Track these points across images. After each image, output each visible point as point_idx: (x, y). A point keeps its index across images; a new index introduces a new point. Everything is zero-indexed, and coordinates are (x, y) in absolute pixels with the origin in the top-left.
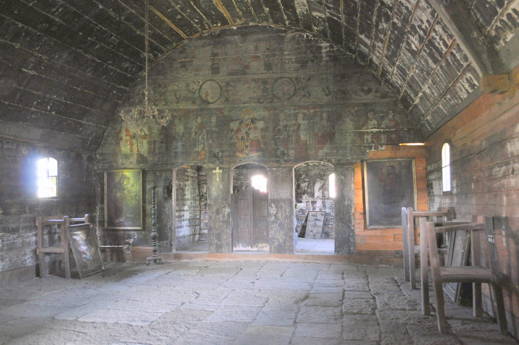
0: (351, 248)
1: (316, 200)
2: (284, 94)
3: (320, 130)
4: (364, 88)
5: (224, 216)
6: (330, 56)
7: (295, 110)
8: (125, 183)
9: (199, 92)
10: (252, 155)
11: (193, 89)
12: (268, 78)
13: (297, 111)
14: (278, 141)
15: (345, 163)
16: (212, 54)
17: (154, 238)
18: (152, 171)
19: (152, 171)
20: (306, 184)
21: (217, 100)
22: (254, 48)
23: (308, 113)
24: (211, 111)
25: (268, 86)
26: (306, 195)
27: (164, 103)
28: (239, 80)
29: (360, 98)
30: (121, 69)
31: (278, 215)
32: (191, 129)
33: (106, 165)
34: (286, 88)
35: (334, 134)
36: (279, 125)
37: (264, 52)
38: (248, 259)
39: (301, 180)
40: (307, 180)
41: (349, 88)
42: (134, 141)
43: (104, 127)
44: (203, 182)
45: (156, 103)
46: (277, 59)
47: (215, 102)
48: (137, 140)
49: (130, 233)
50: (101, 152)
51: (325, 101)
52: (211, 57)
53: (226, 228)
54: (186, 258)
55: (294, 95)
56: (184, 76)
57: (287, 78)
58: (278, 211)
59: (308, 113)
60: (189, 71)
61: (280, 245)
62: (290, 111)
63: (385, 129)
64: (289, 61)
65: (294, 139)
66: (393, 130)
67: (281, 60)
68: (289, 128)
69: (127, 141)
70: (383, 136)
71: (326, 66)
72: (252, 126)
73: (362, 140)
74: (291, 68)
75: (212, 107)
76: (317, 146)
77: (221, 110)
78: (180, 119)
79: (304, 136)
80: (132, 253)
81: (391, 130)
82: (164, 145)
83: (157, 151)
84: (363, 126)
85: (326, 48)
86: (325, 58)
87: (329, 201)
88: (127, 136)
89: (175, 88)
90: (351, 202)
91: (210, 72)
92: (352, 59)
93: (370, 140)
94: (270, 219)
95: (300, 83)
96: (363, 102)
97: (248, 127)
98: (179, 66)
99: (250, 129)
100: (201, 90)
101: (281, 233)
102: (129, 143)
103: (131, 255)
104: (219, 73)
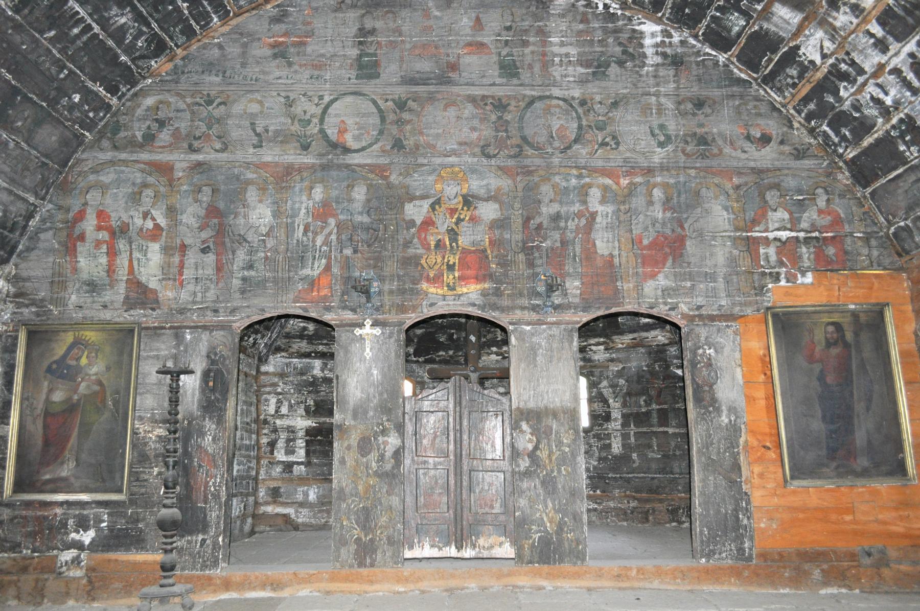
0: (743, 543)
2: (552, 137)
3: (646, 229)
4: (753, 133)
5: (382, 458)
6: (664, 55)
7: (580, 177)
8: (84, 361)
9: (322, 121)
10: (465, 290)
11: (305, 112)
12: (509, 97)
13: (587, 180)
14: (537, 255)
15: (717, 316)
16: (360, 29)
18: (171, 328)
19: (171, 328)
21: (370, 145)
22: (472, 24)
23: (615, 187)
24: (354, 171)
25: (508, 117)
27: (218, 146)
28: (431, 98)
29: (744, 156)
30: (104, 23)
31: (538, 453)
32: (294, 215)
33: (26, 311)
34: (556, 124)
35: (681, 241)
36: (540, 214)
37: (499, 35)
38: (453, 583)
41: (715, 130)
43: (32, 199)
44: (268, 389)
45: (196, 144)
46: (533, 52)
47: (363, 149)
48: (130, 243)
50: (14, 272)
51: (656, 159)
52: (356, 36)
55: (576, 141)
56: (280, 78)
57: (558, 98)
58: (538, 442)
59: (615, 187)
60: (296, 67)
61: (545, 542)
62: (568, 181)
63: (810, 232)
64: (561, 60)
65: (578, 250)
66: (830, 234)
67: (544, 54)
68: (566, 222)
69: (98, 244)
70: (804, 249)
71: (655, 77)
72: (466, 215)
73: (755, 257)
74: (566, 76)
75: (356, 161)
76: (640, 270)
77: (380, 170)
78: (263, 189)
79: (605, 245)
80: (87, 575)
81: (825, 235)
82: (211, 258)
83: (188, 274)
84: (755, 222)
85: (653, 35)
86: (652, 59)
88: (99, 228)
89: (254, 108)
90: (737, 417)
91: (353, 73)
92: (716, 63)
93: (773, 258)
94: (518, 466)
95: (592, 114)
96: (752, 164)
97: (456, 216)
98: (268, 52)
99: (459, 220)
100: (326, 119)
101: (550, 505)
102: (104, 248)
103: (84, 581)
104: (377, 76)
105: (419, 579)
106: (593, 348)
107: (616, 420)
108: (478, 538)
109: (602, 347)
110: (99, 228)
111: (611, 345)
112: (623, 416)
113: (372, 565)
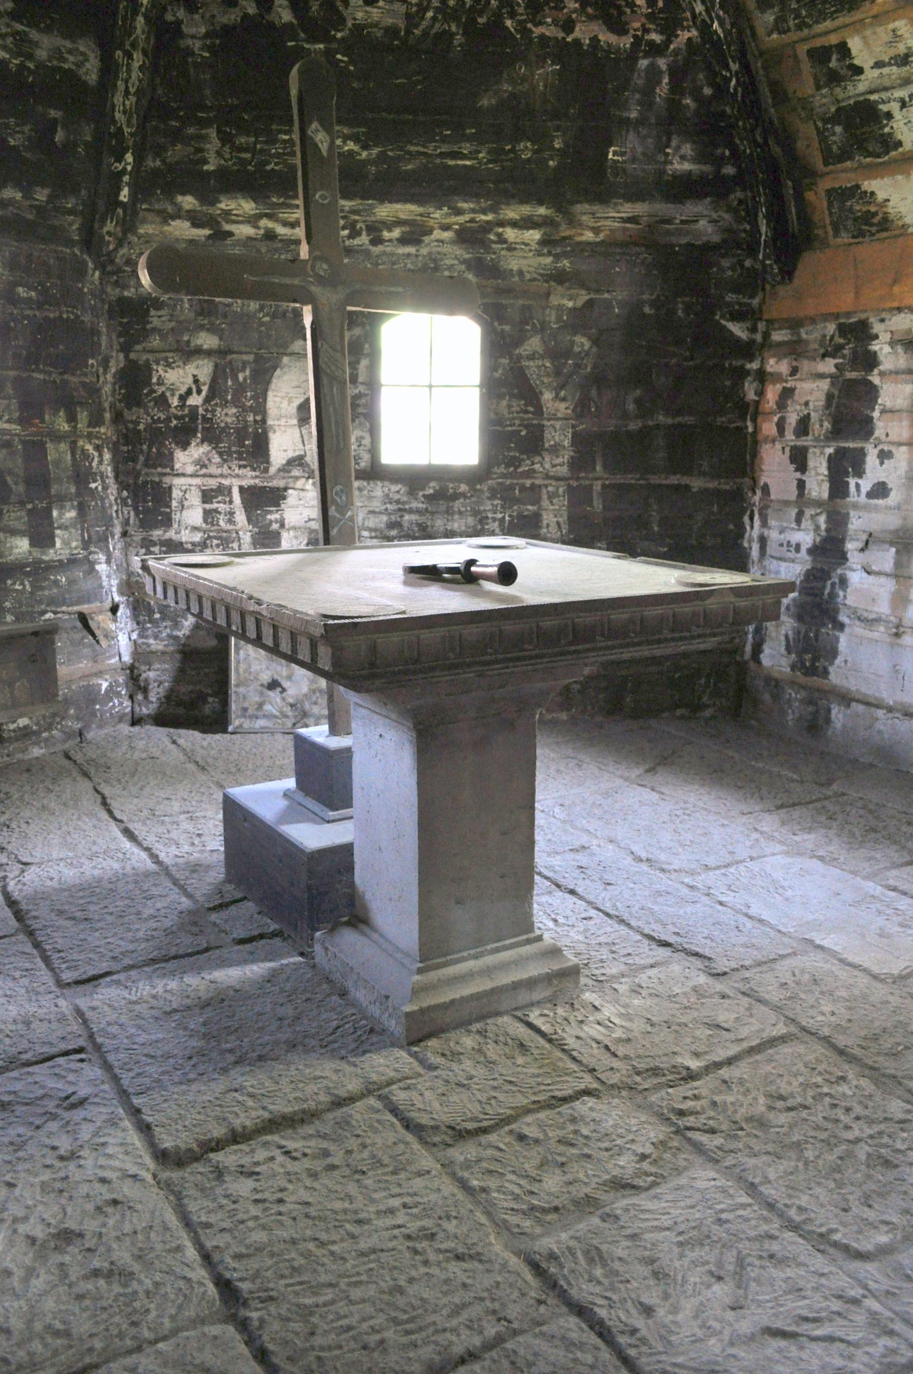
1: (279, 483)
20: (203, 369)
26: (197, 450)
39: (155, 342)
40: (207, 340)
87: (379, 489)
106: (510, 234)
107: (555, 450)
109: (535, 235)
111: (565, 231)
112: (577, 439)
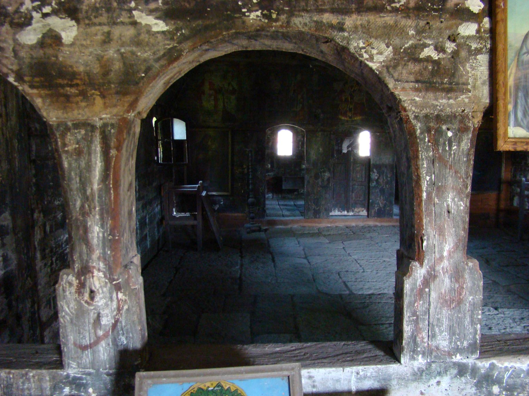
5: (323, 180)
8: (209, 143)
10: (356, 119)
17: (253, 204)
31: (379, 180)
38: (347, 224)
42: (220, 96)
49: (214, 198)
53: (326, 193)
54: (281, 224)
61: (379, 210)
88: (210, 89)
94: (372, 184)
99: (354, 91)
102: (213, 98)
105: (336, 222)
108: (354, 208)
110: (210, 89)
113: (319, 218)
